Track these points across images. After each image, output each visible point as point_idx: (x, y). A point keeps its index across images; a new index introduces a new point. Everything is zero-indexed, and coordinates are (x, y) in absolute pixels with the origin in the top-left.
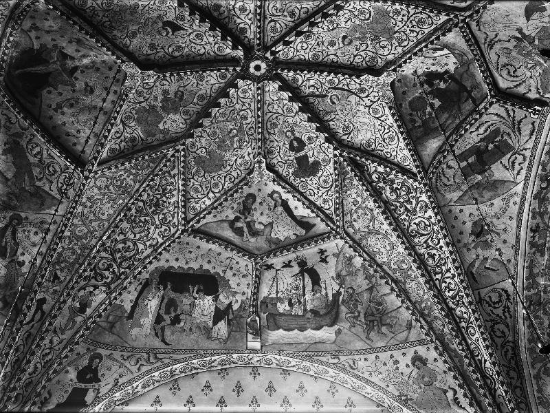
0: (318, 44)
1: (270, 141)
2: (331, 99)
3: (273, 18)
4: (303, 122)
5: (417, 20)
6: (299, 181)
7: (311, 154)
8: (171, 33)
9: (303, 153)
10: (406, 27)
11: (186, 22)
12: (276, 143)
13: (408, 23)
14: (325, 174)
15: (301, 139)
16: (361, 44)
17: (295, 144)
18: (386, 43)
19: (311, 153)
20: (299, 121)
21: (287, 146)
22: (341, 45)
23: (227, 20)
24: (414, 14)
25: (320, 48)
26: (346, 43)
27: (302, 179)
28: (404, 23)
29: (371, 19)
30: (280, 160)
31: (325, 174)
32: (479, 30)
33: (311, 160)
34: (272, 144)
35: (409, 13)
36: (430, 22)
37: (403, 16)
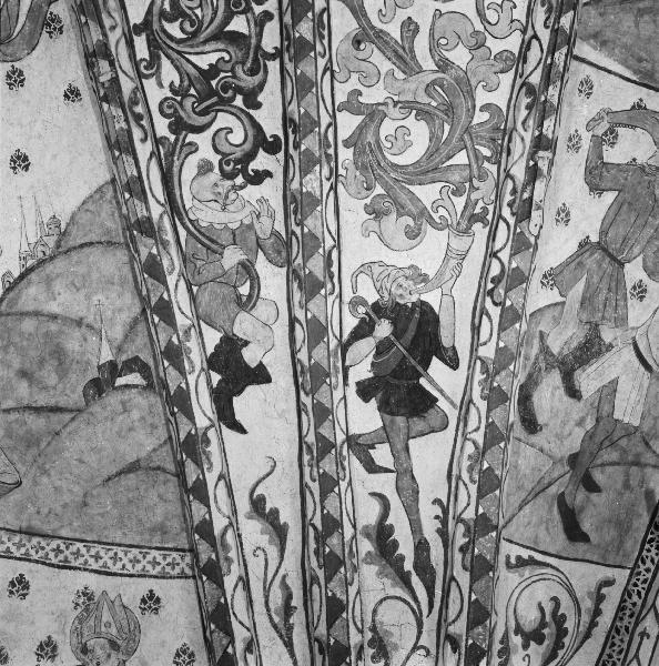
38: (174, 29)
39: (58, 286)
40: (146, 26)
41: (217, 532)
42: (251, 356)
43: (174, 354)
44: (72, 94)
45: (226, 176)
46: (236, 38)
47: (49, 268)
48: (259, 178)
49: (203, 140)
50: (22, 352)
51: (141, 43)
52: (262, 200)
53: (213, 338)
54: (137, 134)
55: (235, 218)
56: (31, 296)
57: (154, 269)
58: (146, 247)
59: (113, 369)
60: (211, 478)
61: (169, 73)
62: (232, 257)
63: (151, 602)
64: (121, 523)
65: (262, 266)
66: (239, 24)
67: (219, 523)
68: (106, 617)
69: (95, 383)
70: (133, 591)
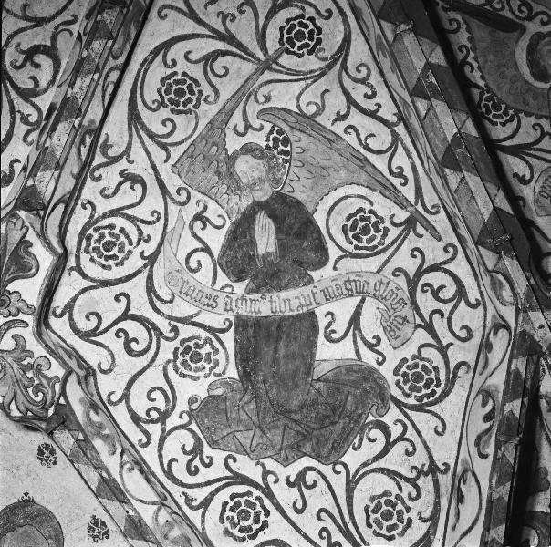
1: (127, 177)
2: (532, 51)
4: (356, 118)
6: (218, 470)
7: (340, 326)
9: (287, 301)
12: (154, 201)
14: (395, 460)
15: (309, 223)
17: (265, 238)
19: (344, 309)
20: (336, 102)
21: (216, 239)
27: (246, 466)
30: (141, 306)
31: (395, 460)
33: (329, 354)
34: (128, 196)
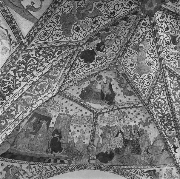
0: (108, 7)
3: (126, 27)
5: (48, 35)
8: (178, 37)
10: (54, 27)
11: (167, 40)
13: (52, 30)
16: (81, 5)
18: (66, 10)
22: (94, 4)
23: (148, 33)
24: (49, 38)
25: (107, 3)
26: (91, 5)
28: (55, 30)
29: (73, 26)
32: (7, 30)
35: (52, 37)
36: (40, 37)
37: (55, 34)
38: (163, 121)
39: (157, 143)
40: (160, 121)
41: (178, 163)
42: (176, 146)
43: (170, 149)
44: (154, 128)
45: (170, 131)
46: (169, 120)
47: (156, 142)
48: (173, 131)
49: (167, 129)
50: (155, 150)
51: (160, 123)
52: (174, 132)
53: (172, 145)
54: (163, 132)
55: (172, 134)
56: (155, 145)
57: (167, 142)
58: (165, 141)
59: (164, 149)
60: (176, 159)
61: (163, 124)
62: (172, 138)
63: (172, 169)
64: (168, 162)
65: (176, 138)
66: (169, 119)
67: (178, 162)
68: (169, 171)
69: (162, 151)
70: (171, 168)
